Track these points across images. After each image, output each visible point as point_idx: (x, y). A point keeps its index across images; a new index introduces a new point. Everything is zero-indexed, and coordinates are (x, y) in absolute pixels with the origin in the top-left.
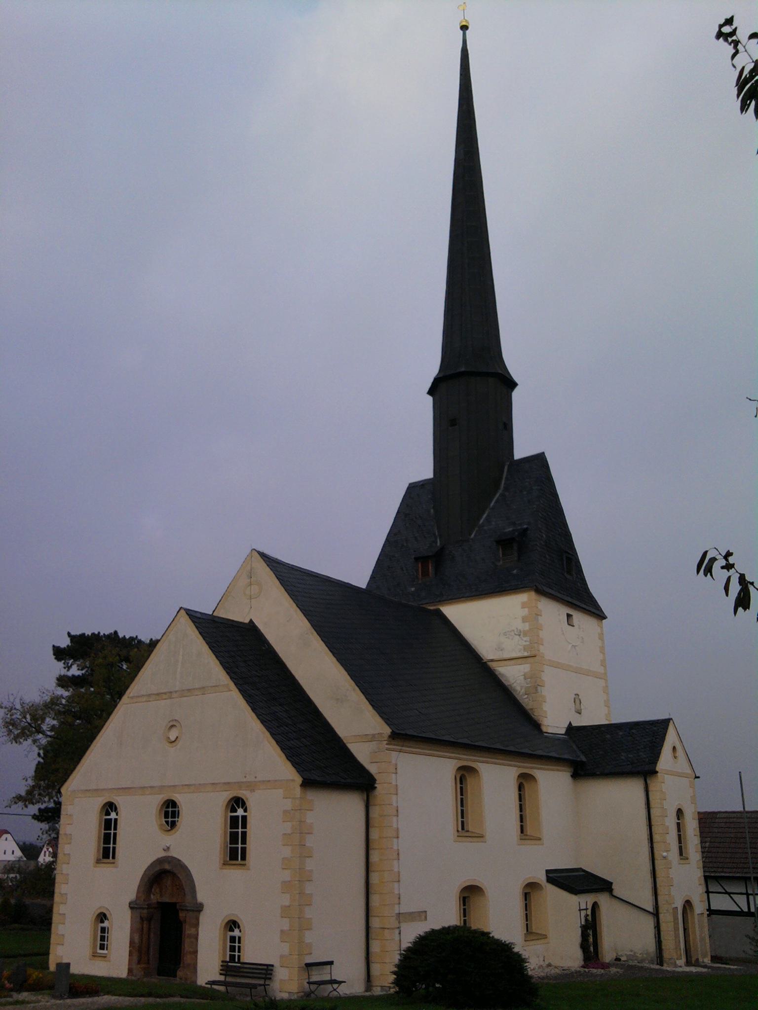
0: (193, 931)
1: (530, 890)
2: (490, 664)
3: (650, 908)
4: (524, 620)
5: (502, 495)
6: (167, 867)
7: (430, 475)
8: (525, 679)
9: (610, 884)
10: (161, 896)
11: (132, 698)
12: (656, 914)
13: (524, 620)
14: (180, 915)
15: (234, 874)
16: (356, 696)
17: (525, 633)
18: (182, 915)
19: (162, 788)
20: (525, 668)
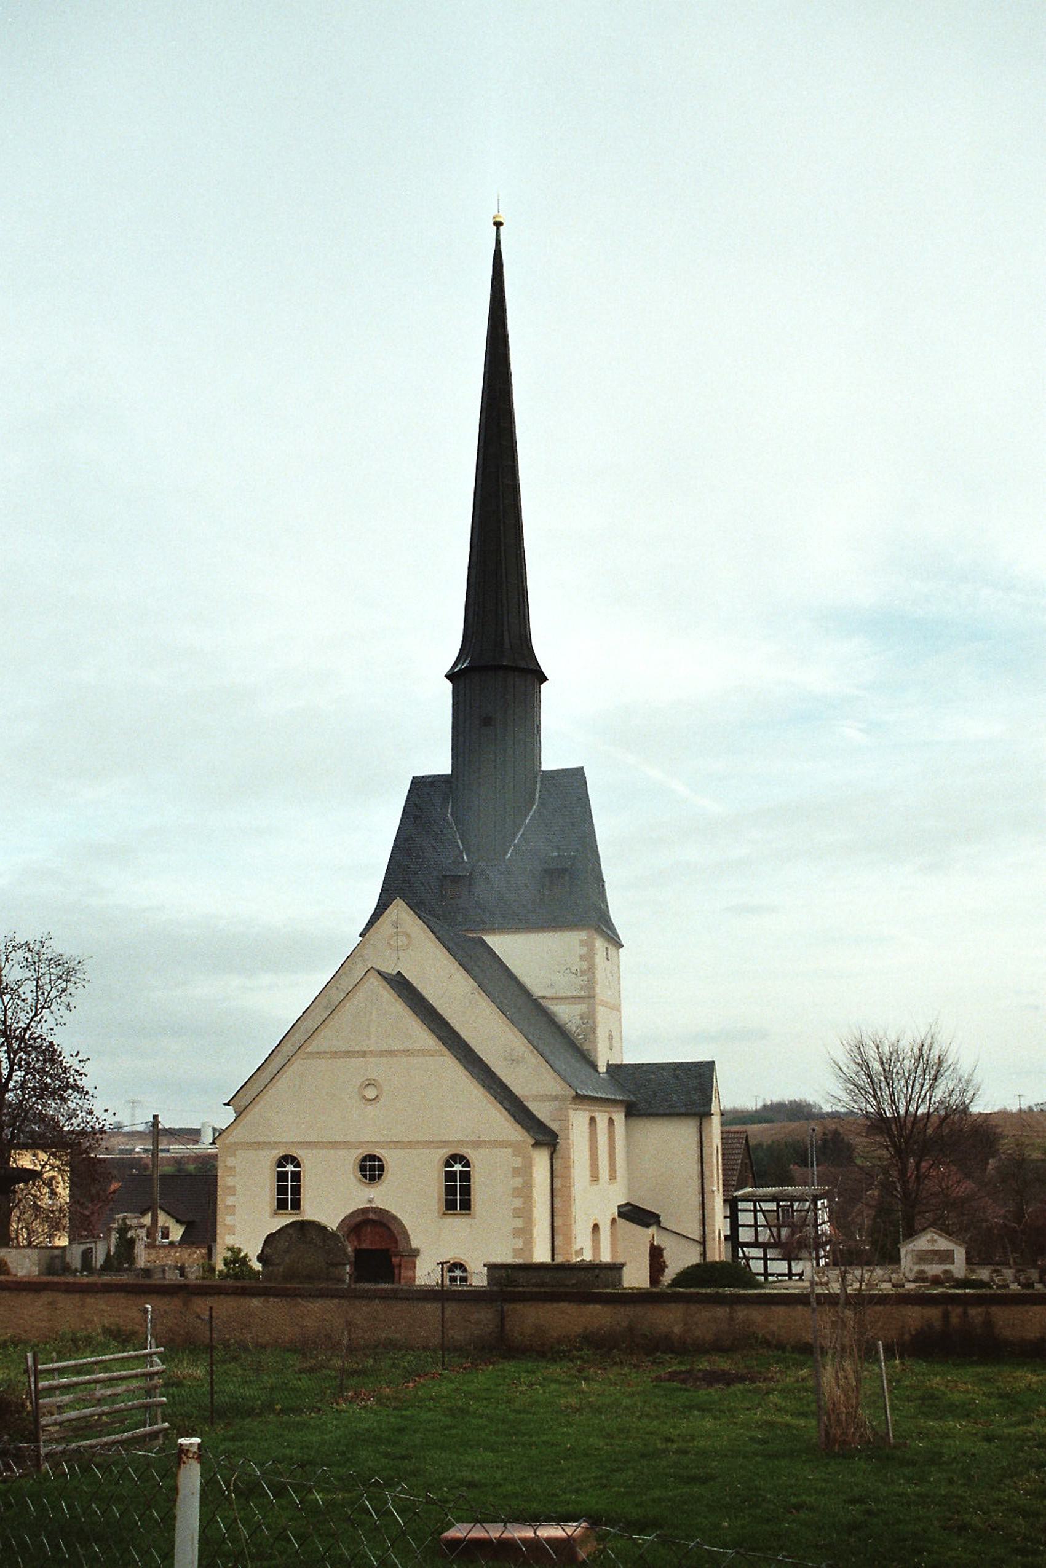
0: (410, 1273)
1: (614, 1221)
2: (541, 1001)
3: (697, 1236)
4: (582, 957)
5: (538, 811)
6: (371, 1216)
7: (450, 772)
8: (581, 1018)
9: (658, 1216)
10: (359, 1241)
11: (311, 1053)
12: (703, 1243)
13: (582, 958)
14: (393, 1259)
15: (457, 1223)
16: (533, 1060)
17: (583, 972)
18: (395, 1260)
19: (362, 1144)
20: (580, 1008)
